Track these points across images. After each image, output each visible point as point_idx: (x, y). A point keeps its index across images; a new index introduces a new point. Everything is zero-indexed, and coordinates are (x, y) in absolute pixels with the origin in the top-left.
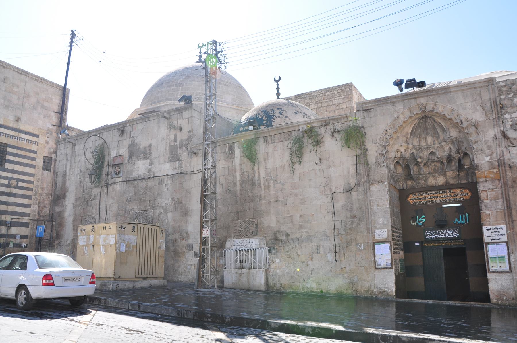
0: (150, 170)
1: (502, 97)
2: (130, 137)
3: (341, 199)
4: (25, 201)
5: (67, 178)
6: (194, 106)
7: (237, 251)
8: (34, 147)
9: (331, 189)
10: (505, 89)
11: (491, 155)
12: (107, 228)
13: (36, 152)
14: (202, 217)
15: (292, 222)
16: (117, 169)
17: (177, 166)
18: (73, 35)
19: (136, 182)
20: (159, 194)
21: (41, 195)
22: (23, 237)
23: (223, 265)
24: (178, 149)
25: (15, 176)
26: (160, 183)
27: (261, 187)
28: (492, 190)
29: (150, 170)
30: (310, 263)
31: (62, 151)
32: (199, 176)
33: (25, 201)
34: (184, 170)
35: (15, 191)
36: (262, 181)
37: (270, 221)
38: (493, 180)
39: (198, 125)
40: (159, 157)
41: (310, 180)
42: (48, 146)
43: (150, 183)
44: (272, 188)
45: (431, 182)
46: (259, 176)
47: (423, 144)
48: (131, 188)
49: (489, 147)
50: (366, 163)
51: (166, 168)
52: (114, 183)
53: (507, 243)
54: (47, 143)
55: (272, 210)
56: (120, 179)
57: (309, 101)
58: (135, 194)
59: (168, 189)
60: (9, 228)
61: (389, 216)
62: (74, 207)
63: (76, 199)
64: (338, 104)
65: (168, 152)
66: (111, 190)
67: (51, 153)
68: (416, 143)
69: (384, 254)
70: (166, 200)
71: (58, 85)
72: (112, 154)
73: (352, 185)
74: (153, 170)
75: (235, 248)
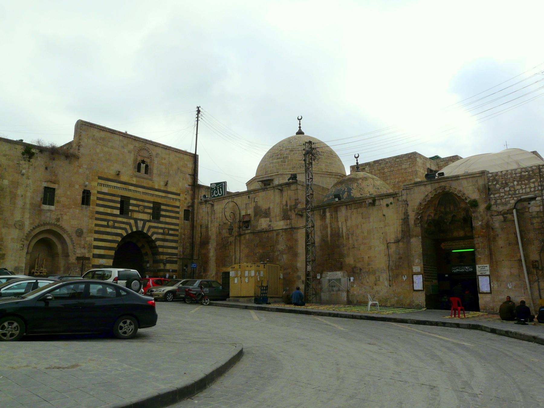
0: (270, 225)
1: (490, 183)
3: (393, 248)
6: (298, 182)
7: (329, 281)
8: (177, 204)
9: (387, 241)
10: (491, 178)
11: (482, 221)
12: (249, 266)
13: (178, 207)
14: (306, 259)
15: (363, 261)
16: (246, 224)
18: (199, 111)
21: (184, 239)
22: (174, 271)
23: (321, 289)
25: (167, 226)
26: (277, 235)
28: (482, 242)
29: (270, 225)
30: (374, 287)
31: (204, 210)
32: (304, 231)
34: (293, 226)
35: (168, 237)
36: (344, 235)
37: (349, 260)
39: (302, 195)
42: (187, 202)
43: (270, 235)
44: (350, 239)
45: (455, 234)
46: (342, 231)
47: (448, 210)
50: (409, 225)
51: (280, 225)
52: (245, 234)
53: (489, 276)
54: (186, 199)
61: (422, 258)
62: (215, 250)
63: (217, 245)
64: (405, 169)
67: (189, 207)
68: (443, 210)
69: (418, 282)
70: (281, 247)
75: (328, 278)
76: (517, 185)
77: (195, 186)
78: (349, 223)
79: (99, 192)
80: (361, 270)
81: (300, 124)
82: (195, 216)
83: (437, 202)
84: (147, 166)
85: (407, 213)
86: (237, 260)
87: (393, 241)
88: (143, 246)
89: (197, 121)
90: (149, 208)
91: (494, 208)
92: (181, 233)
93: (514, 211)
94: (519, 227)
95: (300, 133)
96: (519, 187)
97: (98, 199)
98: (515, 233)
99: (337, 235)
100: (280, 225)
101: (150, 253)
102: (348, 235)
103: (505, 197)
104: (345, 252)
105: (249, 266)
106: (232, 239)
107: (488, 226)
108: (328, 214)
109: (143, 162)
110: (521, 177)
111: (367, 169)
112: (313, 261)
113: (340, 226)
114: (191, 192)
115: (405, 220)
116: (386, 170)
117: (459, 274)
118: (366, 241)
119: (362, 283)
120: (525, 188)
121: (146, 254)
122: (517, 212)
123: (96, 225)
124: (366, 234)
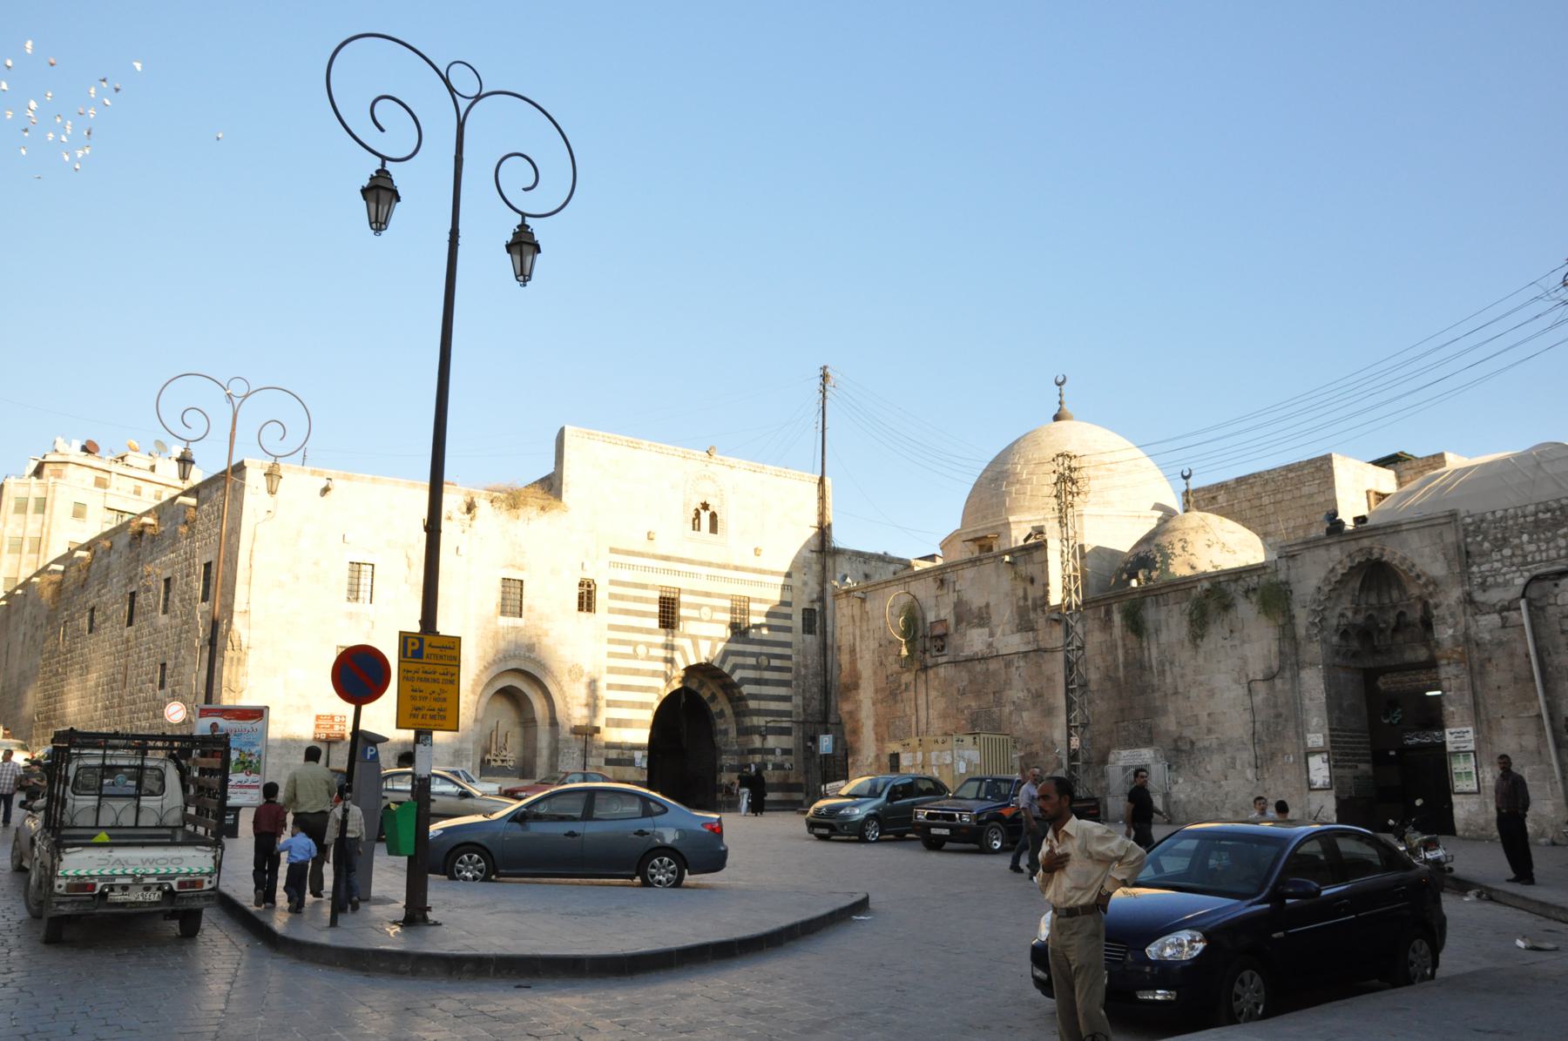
0: (990, 645)
3: (1261, 690)
4: (782, 691)
14: (1069, 721)
16: (939, 643)
18: (825, 377)
20: (1008, 683)
21: (805, 677)
22: (786, 752)
23: (1107, 788)
26: (1008, 665)
33: (782, 691)
34: (1042, 645)
35: (767, 675)
36: (1154, 663)
37: (1169, 724)
38: (1458, 663)
42: (807, 590)
43: (993, 665)
44: (1168, 674)
45: (1409, 656)
47: (1387, 601)
49: (1452, 615)
52: (937, 665)
54: (805, 584)
55: (1170, 708)
56: (944, 659)
58: (971, 682)
60: (764, 738)
62: (874, 704)
63: (876, 691)
64: (1311, 496)
68: (1373, 600)
69: (1319, 770)
70: (1016, 693)
73: (1275, 669)
75: (1121, 763)
79: (612, 582)
80: (1192, 743)
82: (829, 622)
83: (1358, 585)
84: (713, 516)
86: (923, 726)
87: (1260, 676)
88: (713, 698)
90: (724, 610)
92: (798, 664)
93: (1523, 603)
96: (1532, 547)
97: (613, 596)
98: (1527, 655)
100: (1013, 642)
101: (728, 711)
102: (1162, 663)
109: (705, 506)
110: (1537, 524)
111: (1222, 498)
112: (1084, 726)
114: (816, 568)
116: (1265, 500)
117: (1420, 747)
118: (1201, 678)
119: (1196, 774)
120: (1547, 550)
121: (721, 714)
122: (1529, 604)
123: (611, 655)
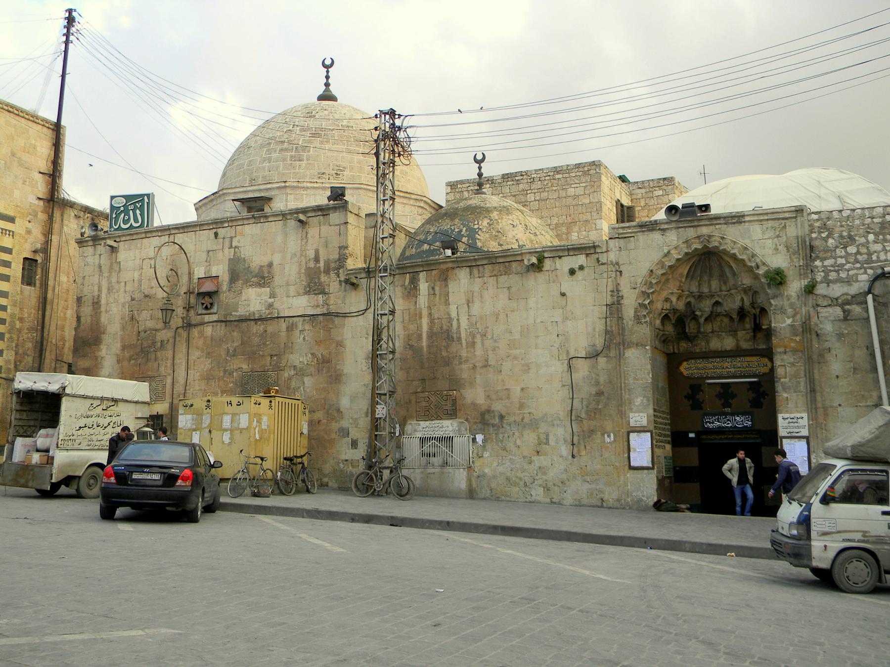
0: (270, 306)
1: (814, 235)
2: (231, 247)
3: (583, 368)
5: (103, 309)
6: (350, 207)
7: (423, 440)
9: (568, 352)
11: (794, 316)
12: (234, 403)
13: (9, 251)
15: (508, 397)
16: (207, 300)
17: (321, 302)
18: (70, 20)
19: (244, 325)
20: (289, 347)
21: (20, 331)
24: (322, 275)
26: (290, 329)
27: (461, 343)
28: (793, 364)
29: (270, 306)
30: (535, 458)
31: (90, 260)
34: (333, 309)
36: (463, 335)
37: (475, 395)
38: (795, 351)
39: (356, 238)
40: (288, 285)
41: (537, 337)
42: (31, 239)
43: (271, 328)
44: (478, 346)
45: (715, 344)
47: (705, 290)
48: (235, 334)
49: (792, 305)
50: (620, 318)
52: (203, 324)
53: (807, 438)
54: (29, 232)
55: (479, 380)
57: (527, 187)
59: (304, 338)
61: (650, 394)
62: (118, 362)
63: (124, 348)
64: (576, 197)
65: (304, 278)
66: (197, 335)
67: (35, 252)
68: (694, 289)
69: (642, 449)
70: (299, 357)
71: (46, 121)
72: (196, 272)
73: (599, 348)
74: (276, 305)
75: (419, 435)
76: (875, 242)
77: (54, 201)
78: (476, 309)
80: (502, 417)
81: (327, 77)
82: (51, 275)
83: (686, 272)
85: (618, 291)
86: (179, 388)
87: (583, 354)
89: (67, 43)
91: (821, 289)
92: (12, 316)
93: (870, 298)
94: (880, 333)
95: (327, 96)
96: (878, 247)
98: (870, 347)
99: (444, 335)
103: (848, 266)
104: (465, 375)
105: (234, 403)
106: (165, 335)
107: (807, 329)
108: (423, 286)
112: (392, 393)
113: (454, 314)
114: (42, 217)
115: (615, 307)
117: (720, 431)
118: (516, 352)
119: (505, 449)
124: (517, 335)
